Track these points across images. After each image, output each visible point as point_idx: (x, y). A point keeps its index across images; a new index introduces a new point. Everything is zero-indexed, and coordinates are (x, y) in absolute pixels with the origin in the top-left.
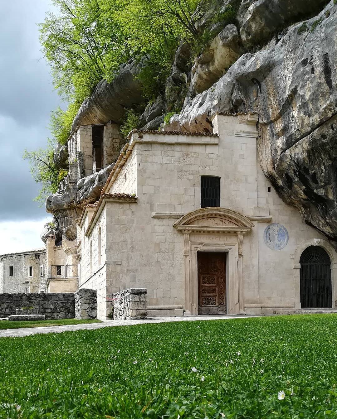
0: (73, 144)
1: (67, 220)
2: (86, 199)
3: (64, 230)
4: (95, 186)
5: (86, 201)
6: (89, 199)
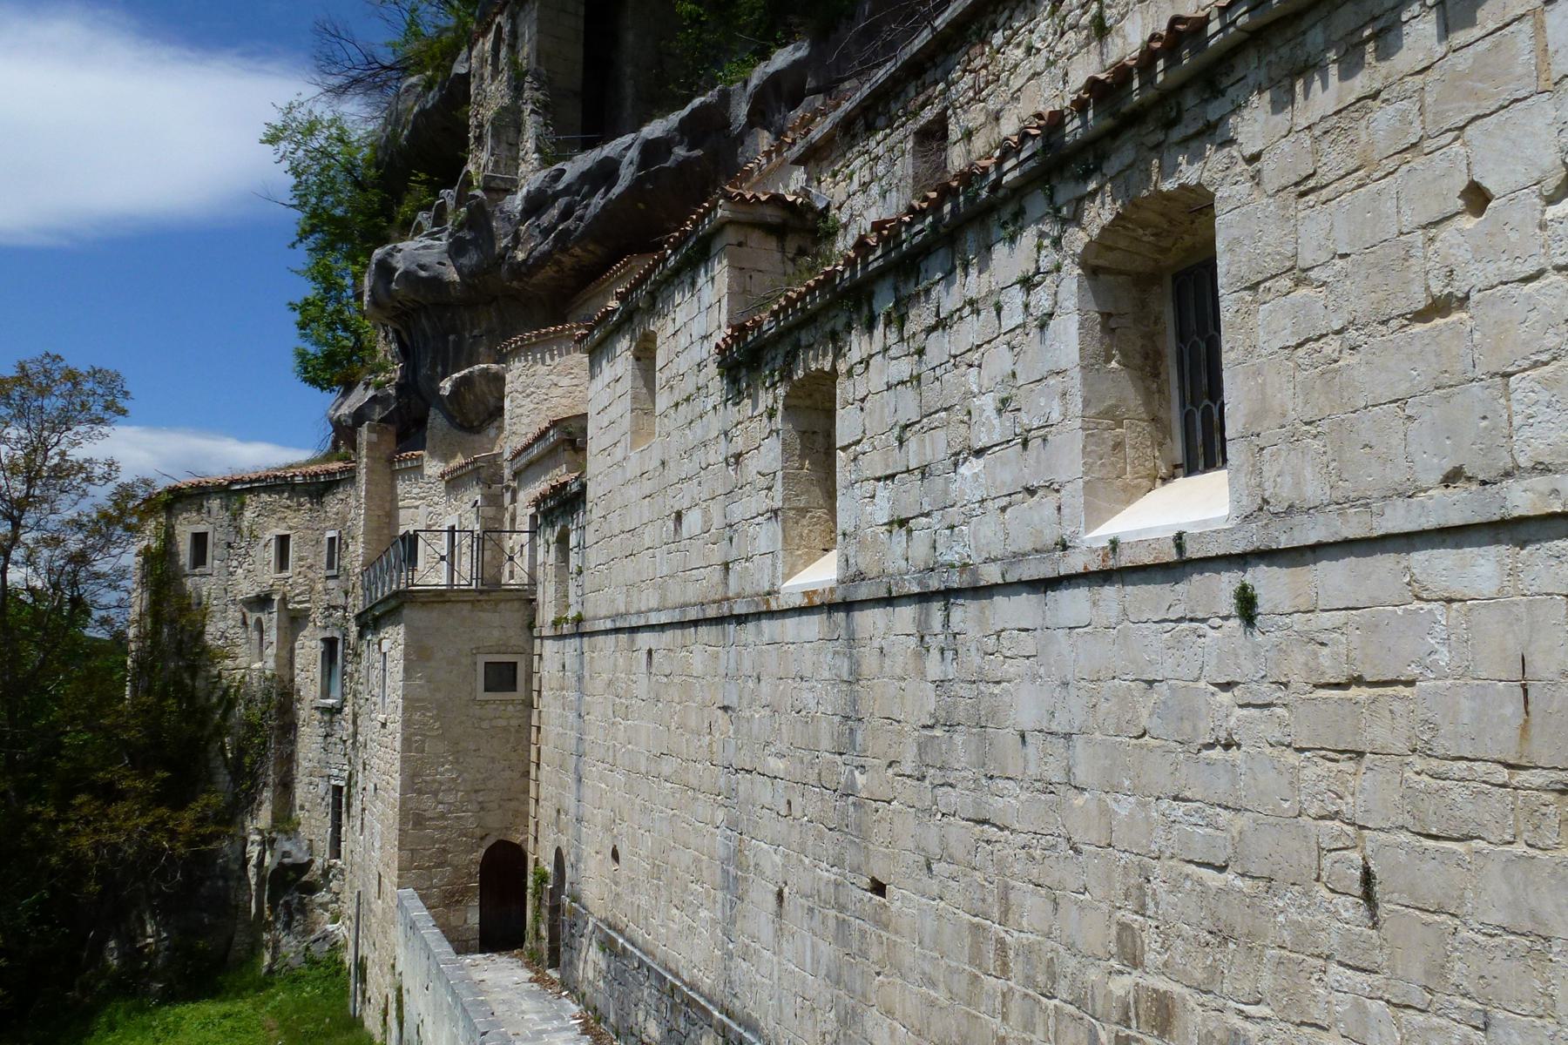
1: (458, 345)
3: (446, 386)
4: (616, 190)
5: (558, 263)
6: (577, 251)
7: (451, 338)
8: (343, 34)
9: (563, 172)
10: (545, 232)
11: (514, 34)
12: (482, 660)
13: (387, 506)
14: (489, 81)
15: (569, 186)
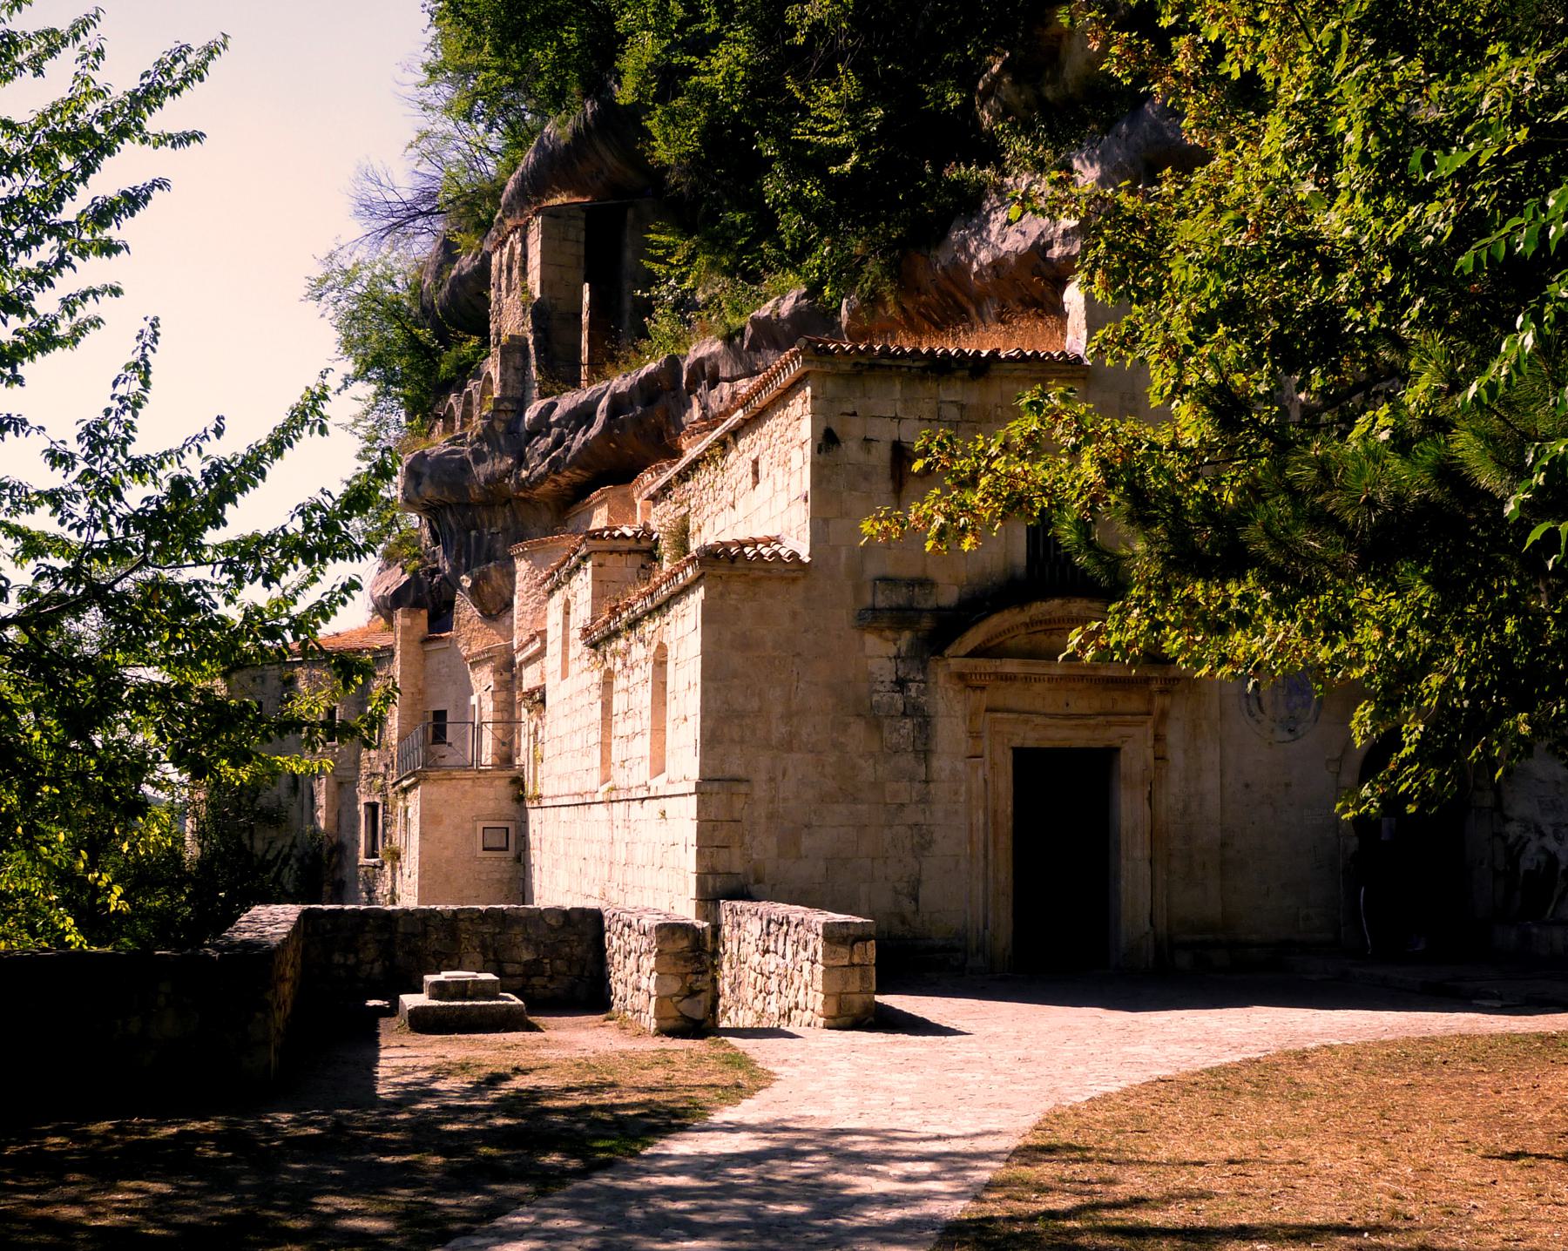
0: (510, 270)
1: (479, 539)
2: (557, 472)
4: (593, 432)
5: (554, 481)
7: (473, 533)
8: (384, 181)
9: (553, 406)
10: (544, 455)
11: (524, 255)
12: (480, 826)
13: (420, 684)
14: (504, 294)
15: (558, 420)
